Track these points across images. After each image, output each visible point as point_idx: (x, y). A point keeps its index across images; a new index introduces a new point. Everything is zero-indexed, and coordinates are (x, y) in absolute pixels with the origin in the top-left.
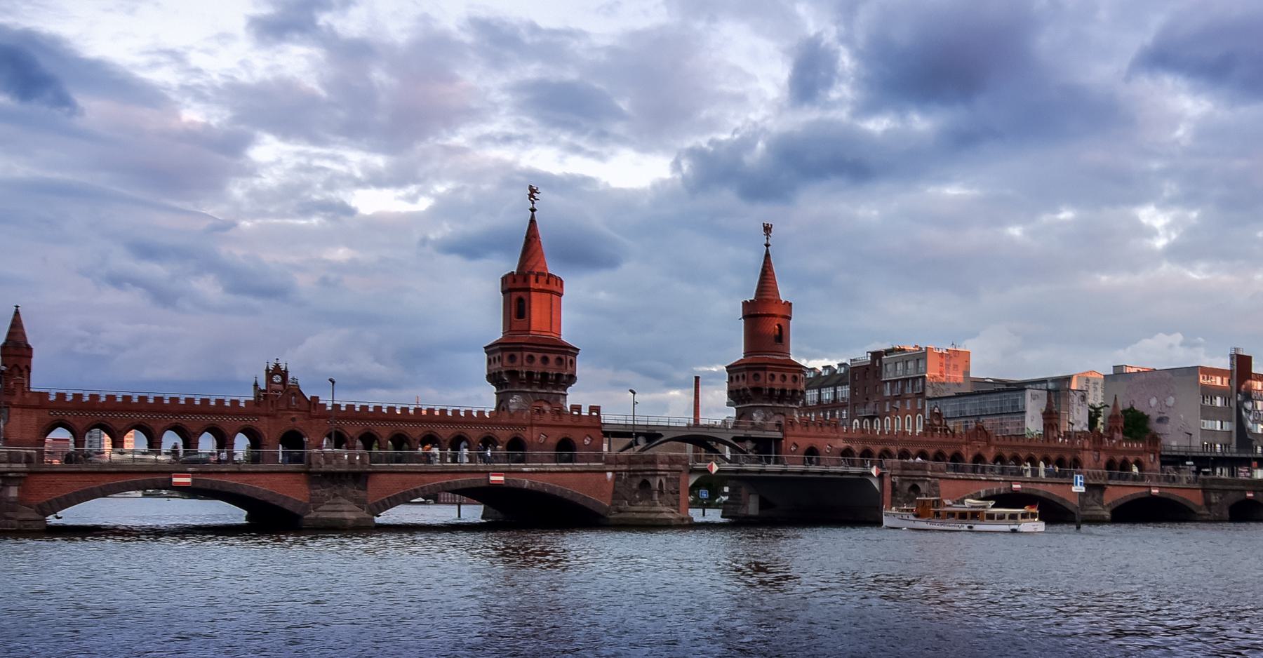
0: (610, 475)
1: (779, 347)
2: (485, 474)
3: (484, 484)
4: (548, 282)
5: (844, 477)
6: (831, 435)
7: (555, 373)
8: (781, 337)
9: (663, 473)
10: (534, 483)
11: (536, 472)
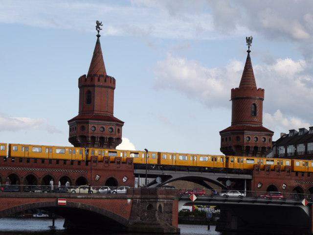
0: (129, 201)
1: (256, 119)
2: (55, 199)
3: (55, 205)
4: (105, 81)
5: (269, 204)
6: (286, 177)
7: (108, 137)
8: (256, 111)
9: (161, 200)
10: (83, 205)
11: (85, 198)
